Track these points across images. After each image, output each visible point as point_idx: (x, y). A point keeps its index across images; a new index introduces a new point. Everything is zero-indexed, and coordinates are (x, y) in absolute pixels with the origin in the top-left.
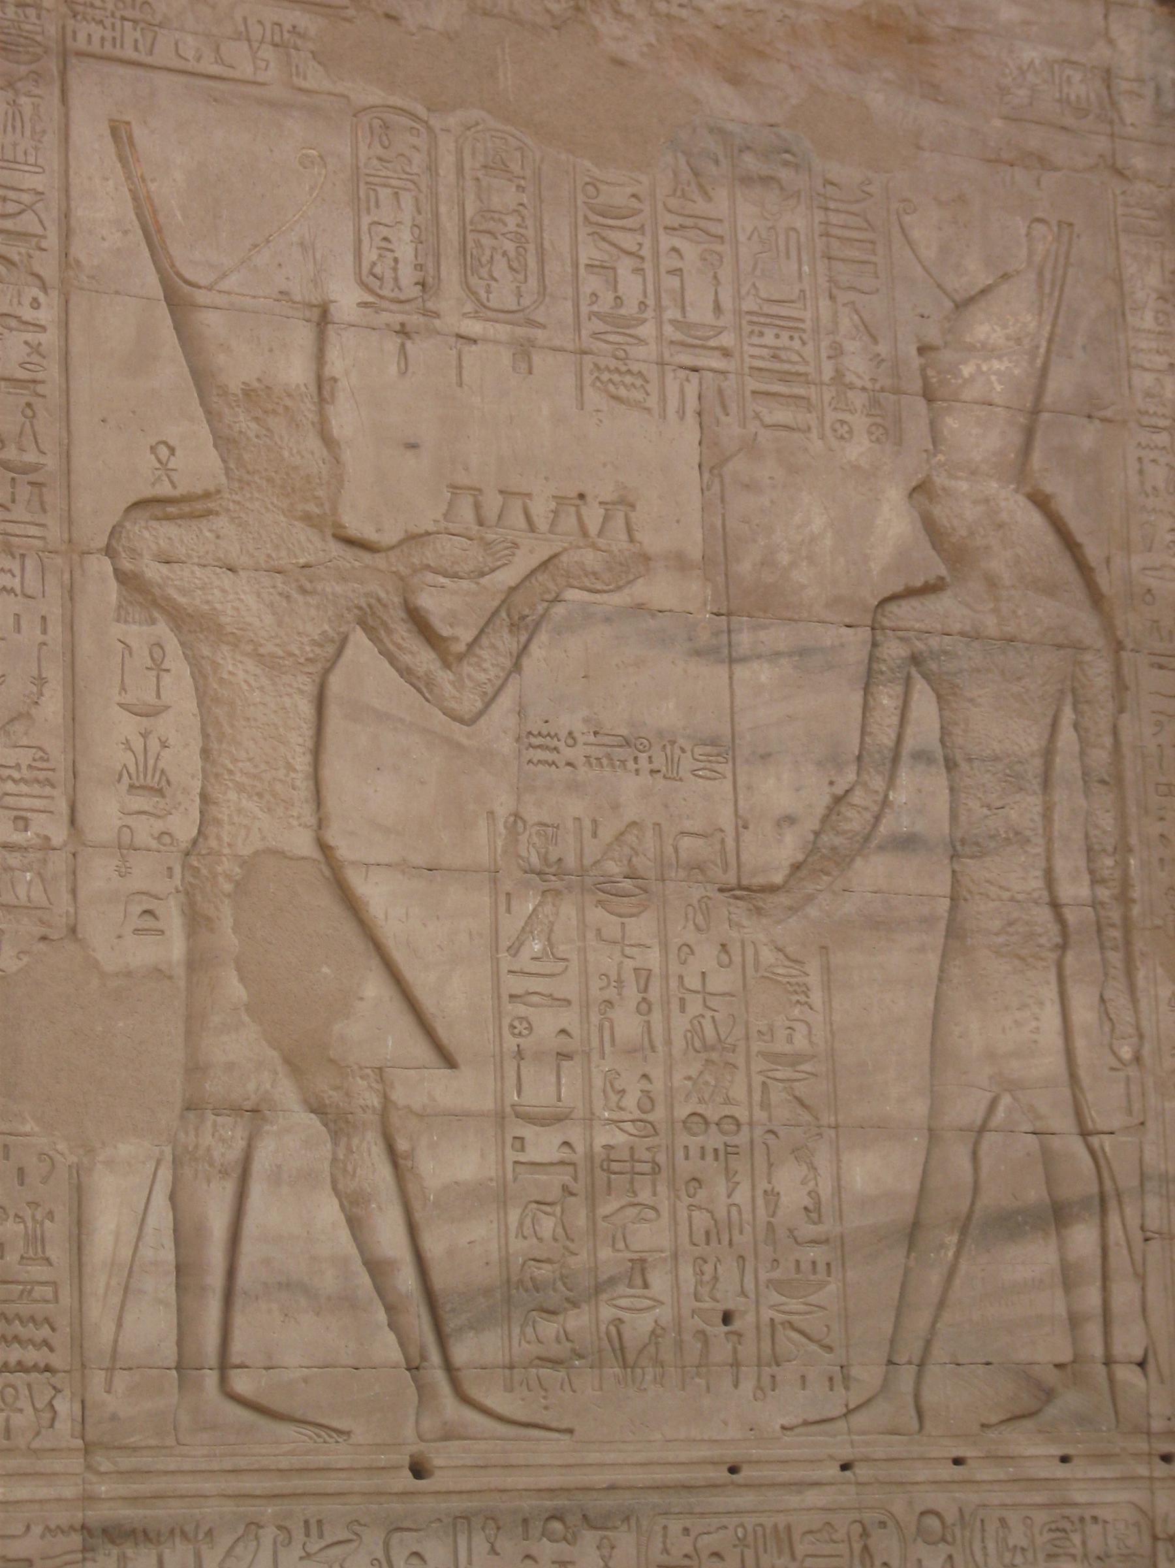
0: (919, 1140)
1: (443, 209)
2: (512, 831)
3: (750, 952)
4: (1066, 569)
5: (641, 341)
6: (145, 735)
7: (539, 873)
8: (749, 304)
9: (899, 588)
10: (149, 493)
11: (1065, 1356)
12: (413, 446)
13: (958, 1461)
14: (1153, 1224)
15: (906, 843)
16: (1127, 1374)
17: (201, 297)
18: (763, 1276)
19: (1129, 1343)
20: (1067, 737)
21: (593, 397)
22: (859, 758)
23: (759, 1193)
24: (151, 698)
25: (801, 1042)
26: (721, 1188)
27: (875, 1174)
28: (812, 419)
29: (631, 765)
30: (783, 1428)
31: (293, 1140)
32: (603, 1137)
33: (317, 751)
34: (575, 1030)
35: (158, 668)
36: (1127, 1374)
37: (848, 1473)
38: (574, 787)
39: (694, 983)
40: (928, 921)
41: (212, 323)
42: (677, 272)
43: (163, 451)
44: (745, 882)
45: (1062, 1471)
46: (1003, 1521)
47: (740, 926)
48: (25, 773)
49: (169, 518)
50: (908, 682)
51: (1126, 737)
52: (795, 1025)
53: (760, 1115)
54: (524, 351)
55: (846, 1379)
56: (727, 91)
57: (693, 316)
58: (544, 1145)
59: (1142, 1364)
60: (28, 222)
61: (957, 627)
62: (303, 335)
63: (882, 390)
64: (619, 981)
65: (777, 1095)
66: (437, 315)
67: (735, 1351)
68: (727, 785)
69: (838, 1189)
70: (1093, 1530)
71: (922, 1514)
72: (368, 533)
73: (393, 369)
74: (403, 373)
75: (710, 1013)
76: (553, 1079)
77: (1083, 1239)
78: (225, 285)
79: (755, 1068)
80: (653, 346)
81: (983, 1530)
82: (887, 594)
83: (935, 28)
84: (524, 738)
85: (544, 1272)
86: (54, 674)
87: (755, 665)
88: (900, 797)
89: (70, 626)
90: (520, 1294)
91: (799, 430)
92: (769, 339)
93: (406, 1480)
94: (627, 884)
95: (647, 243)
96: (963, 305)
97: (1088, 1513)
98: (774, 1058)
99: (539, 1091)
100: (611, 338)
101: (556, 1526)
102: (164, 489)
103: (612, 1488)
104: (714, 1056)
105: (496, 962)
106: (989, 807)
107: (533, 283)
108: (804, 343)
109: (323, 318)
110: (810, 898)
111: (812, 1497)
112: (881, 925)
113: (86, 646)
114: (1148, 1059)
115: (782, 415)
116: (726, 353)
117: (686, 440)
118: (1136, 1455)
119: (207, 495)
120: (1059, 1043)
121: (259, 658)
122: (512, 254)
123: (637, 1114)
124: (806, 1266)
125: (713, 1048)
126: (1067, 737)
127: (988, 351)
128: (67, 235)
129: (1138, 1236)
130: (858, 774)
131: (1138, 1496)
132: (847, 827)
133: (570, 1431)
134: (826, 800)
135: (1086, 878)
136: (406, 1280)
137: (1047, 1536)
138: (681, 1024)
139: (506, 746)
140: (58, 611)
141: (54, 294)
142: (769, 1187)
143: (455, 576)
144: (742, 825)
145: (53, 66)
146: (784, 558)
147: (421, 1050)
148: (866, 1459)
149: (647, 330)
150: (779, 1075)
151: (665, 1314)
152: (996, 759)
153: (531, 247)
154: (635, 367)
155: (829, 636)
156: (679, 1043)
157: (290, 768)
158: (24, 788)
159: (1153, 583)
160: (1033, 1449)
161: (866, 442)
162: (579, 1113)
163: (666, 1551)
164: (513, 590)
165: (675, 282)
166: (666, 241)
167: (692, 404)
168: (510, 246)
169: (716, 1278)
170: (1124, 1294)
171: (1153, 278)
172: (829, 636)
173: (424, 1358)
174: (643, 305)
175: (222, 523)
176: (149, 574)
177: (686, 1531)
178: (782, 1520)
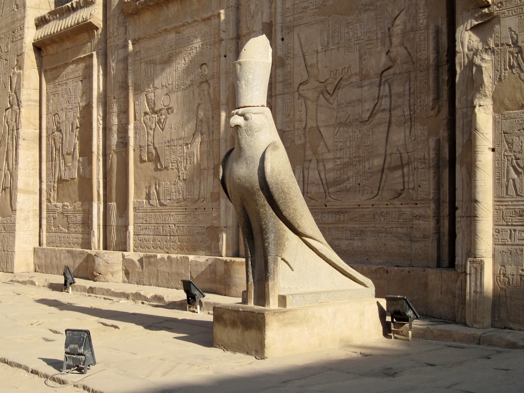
0: (383, 157)
2: (336, 118)
8: (366, 31)
9: (383, 69)
10: (300, 82)
11: (402, 188)
15: (383, 110)
17: (306, 54)
19: (411, 186)
20: (407, 87)
21: (346, 52)
22: (378, 98)
25: (369, 144)
27: (378, 162)
31: (313, 165)
35: (302, 105)
36: (411, 191)
38: (343, 111)
40: (386, 122)
41: (307, 57)
42: (356, 29)
45: (401, 206)
57: (358, 35)
58: (339, 162)
60: (290, 51)
62: (315, 55)
68: (361, 107)
69: (372, 165)
70: (405, 215)
77: (406, 170)
82: (382, 71)
85: (338, 179)
86: (292, 108)
88: (383, 103)
90: (336, 182)
93: (324, 207)
98: (365, 146)
99: (338, 155)
102: (302, 81)
109: (317, 52)
111: (368, 210)
112: (380, 124)
118: (411, 204)
127: (399, 25)
129: (413, 168)
130: (378, 100)
131: (411, 210)
136: (324, 181)
138: (354, 143)
139: (336, 107)
144: (362, 112)
146: (369, 69)
147: (327, 151)
149: (353, 40)
151: (351, 184)
155: (374, 80)
159: (421, 57)
160: (397, 202)
164: (337, 84)
168: (337, 33)
170: (411, 178)
171: (423, 3)
175: (309, 84)
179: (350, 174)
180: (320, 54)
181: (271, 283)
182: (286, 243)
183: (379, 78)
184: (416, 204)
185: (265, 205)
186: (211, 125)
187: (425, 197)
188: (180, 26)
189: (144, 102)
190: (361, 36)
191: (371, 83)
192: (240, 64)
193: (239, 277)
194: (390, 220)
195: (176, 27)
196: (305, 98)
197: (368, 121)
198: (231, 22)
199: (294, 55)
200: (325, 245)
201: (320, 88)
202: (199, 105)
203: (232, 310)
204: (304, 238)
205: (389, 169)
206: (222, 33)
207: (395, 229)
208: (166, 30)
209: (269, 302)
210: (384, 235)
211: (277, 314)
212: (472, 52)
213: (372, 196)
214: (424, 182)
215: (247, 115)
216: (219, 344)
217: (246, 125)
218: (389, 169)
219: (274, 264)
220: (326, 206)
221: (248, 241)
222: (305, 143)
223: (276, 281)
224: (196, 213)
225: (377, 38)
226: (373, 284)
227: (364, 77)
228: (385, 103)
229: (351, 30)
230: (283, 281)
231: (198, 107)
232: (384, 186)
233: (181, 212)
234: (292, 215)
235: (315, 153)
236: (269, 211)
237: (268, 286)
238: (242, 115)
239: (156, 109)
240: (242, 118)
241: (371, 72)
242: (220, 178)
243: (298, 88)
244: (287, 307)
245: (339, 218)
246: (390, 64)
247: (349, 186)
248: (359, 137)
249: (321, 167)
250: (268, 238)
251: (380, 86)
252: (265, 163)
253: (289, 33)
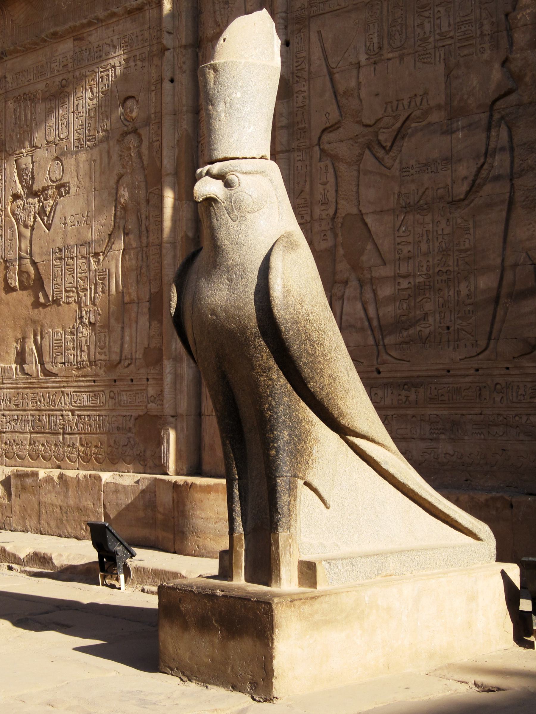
0: (498, 271)
1: (384, 24)
2: (399, 196)
3: (454, 220)
5: (430, 43)
6: (324, 190)
7: (405, 208)
8: (458, 20)
9: (496, 96)
10: (324, 127)
12: (377, 95)
13: (508, 368)
15: (497, 178)
17: (335, 71)
18: (456, 316)
23: (456, 291)
24: (325, 180)
25: (467, 246)
26: (446, 292)
27: (486, 282)
29: (427, 171)
30: (460, 359)
32: (417, 280)
33: (358, 185)
34: (412, 251)
35: (327, 172)
37: (477, 373)
38: (413, 181)
42: (439, 18)
43: (327, 115)
44: (454, 200)
46: (518, 386)
48: (303, 205)
49: (331, 132)
50: (500, 126)
52: (466, 240)
53: (456, 268)
54: (401, 58)
55: (477, 345)
57: (443, 30)
58: (404, 284)
60: (303, 66)
61: (514, 103)
62: (355, 72)
63: (494, 33)
64: (422, 235)
65: (460, 262)
66: (382, 55)
67: (449, 338)
68: (450, 171)
69: (476, 288)
71: (497, 384)
72: (368, 122)
73: (373, 74)
74: (375, 75)
75: (444, 241)
76: (406, 265)
78: (339, 66)
79: (455, 255)
80: (433, 44)
81: (512, 389)
84: (402, 170)
85: (404, 318)
86: (308, 179)
87: (457, 133)
88: (496, 164)
89: (310, 165)
90: (399, 324)
91: (470, 55)
93: (375, 374)
94: (425, 206)
95: (432, 12)
98: (461, 251)
99: (403, 270)
100: (422, 45)
101: (406, 387)
102: (328, 125)
103: (419, 377)
104: (445, 253)
105: (394, 234)
106: (522, 160)
107: (404, 36)
108: (472, 26)
109: (358, 66)
111: (467, 379)
113: (314, 170)
115: (466, 52)
117: (441, 68)
119: (336, 124)
121: (346, 163)
122: (400, 30)
123: (426, 272)
124: (467, 312)
125: (444, 251)
127: (527, 7)
128: (310, 65)
132: (482, 176)
133: (409, 361)
134: (476, 169)
136: (375, 323)
137: (531, 391)
138: (437, 244)
139: (397, 173)
140: (309, 163)
141: (307, 82)
142: (457, 289)
143: (388, 128)
144: (453, 182)
145: (307, 23)
146: (466, 97)
147: (379, 261)
148: (481, 368)
149: (431, 39)
150: (461, 256)
151: (432, 328)
152: (525, 144)
153: (404, 26)
154: (428, 52)
156: (436, 250)
157: (352, 191)
158: (303, 209)
161: (489, 52)
162: (412, 274)
163: (431, 394)
165: (438, 21)
166: (436, 9)
167: (443, 56)
168: (399, 28)
169: (444, 317)
173: (379, 343)
174: (430, 31)
175: (341, 129)
176: (326, 148)
177: (436, 388)
179: (429, 307)
180: (363, 70)
181: (282, 535)
182: (314, 451)
183: (487, 114)
185: (270, 369)
186: (143, 217)
188: (83, 26)
189: (12, 174)
190: (449, 31)
191: (470, 125)
192: (215, 69)
193: (203, 516)
195: (74, 29)
196: (335, 158)
197: (464, 200)
198: (183, 14)
199: (310, 73)
200: (394, 453)
201: (364, 136)
202: (120, 177)
203: (199, 593)
204: (351, 438)
205: (510, 295)
206: (166, 35)
207: (524, 418)
208: (55, 35)
209: (279, 576)
211: (297, 603)
215: (230, 177)
216: (173, 665)
217: (229, 199)
218: (510, 295)
219: (290, 495)
220: (379, 372)
221: (232, 445)
222: (335, 246)
223: (293, 530)
224: (116, 390)
225: (482, 35)
226: (492, 534)
227: (454, 111)
228: (500, 163)
229: (427, 20)
230: (307, 530)
231: (118, 181)
232: (500, 331)
233: (85, 387)
234: (326, 390)
235: (356, 267)
236: (280, 382)
237: (277, 541)
238: (221, 177)
239: (35, 188)
240: (220, 183)
241: (469, 102)
242: (173, 311)
243: (320, 138)
244: (319, 587)
245: (407, 397)
247: (427, 331)
248: (446, 232)
249: (369, 296)
250: (276, 439)
251: (489, 129)
252: (271, 277)
253: (300, 31)
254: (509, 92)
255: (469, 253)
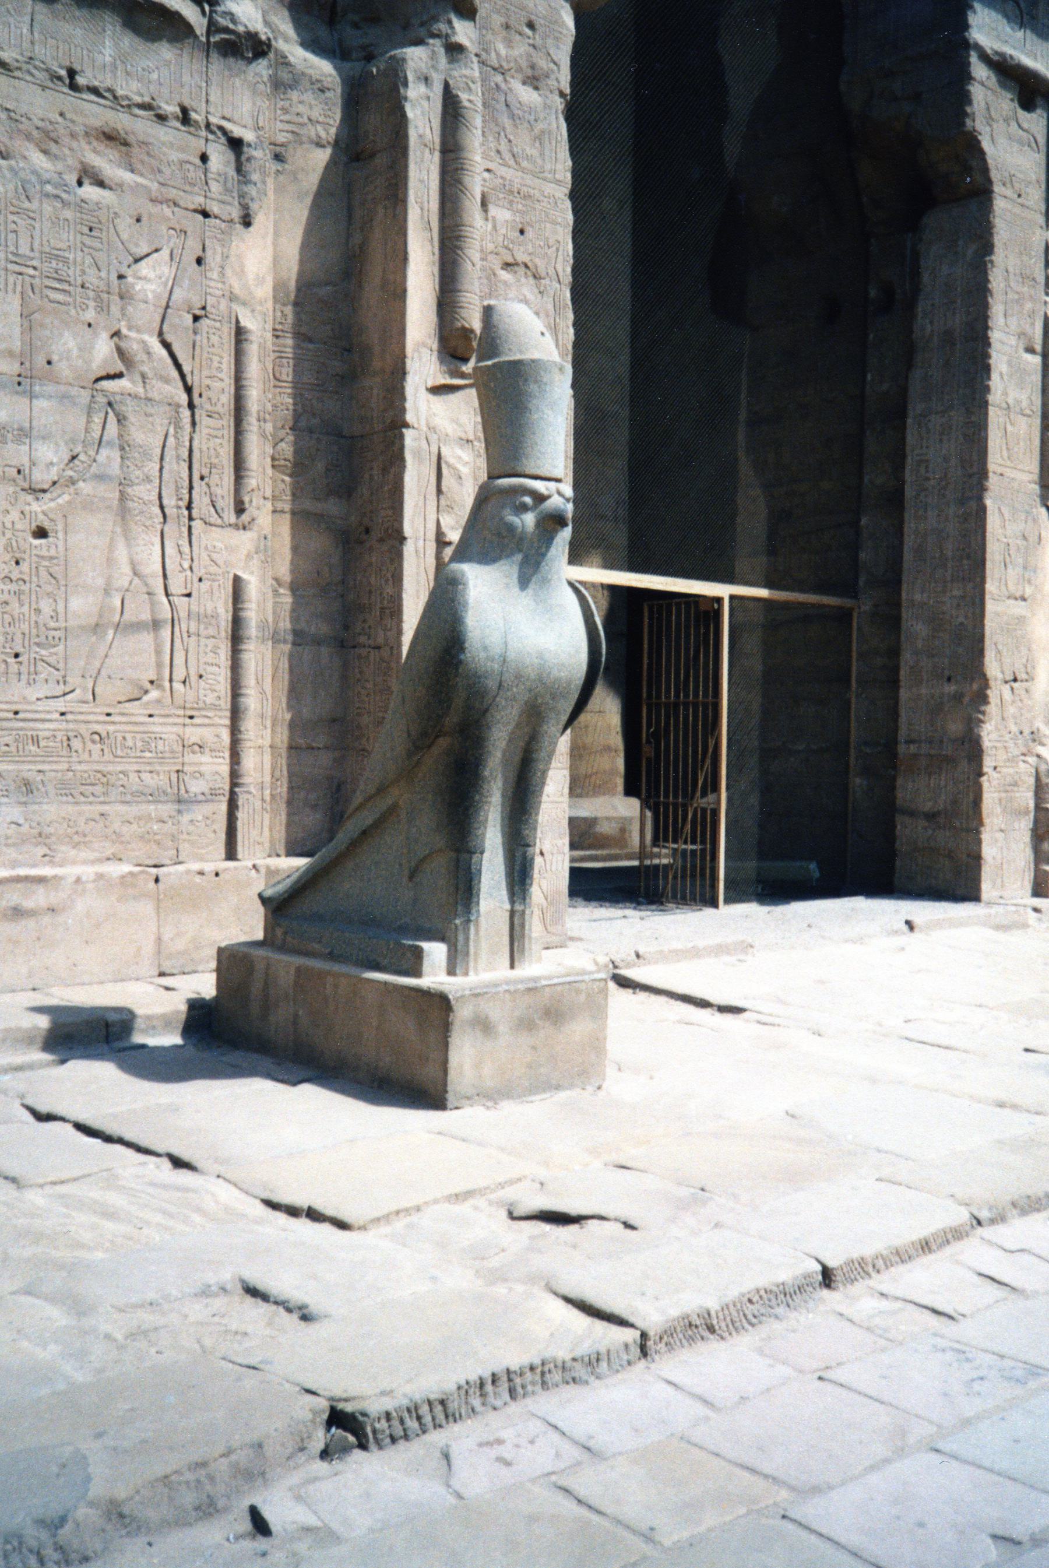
4: (175, 374)
13: (108, 715)
14: (192, 630)
15: (100, 478)
16: (178, 686)
25: (53, 552)
28: (71, 300)
39: (9, 525)
46: (124, 738)
47: (29, 504)
51: (195, 443)
53: (35, 579)
56: (42, 156)
59: (184, 682)
65: (43, 572)
68: (27, 448)
70: (161, 742)
83: (131, 139)
92: (54, 262)
96: (137, 261)
97: (158, 736)
98: (42, 557)
110: (59, 496)
111: (47, 725)
114: (194, 569)
116: (35, 268)
120: (160, 559)
126: (171, 440)
129: (185, 635)
131: (179, 730)
135: (175, 498)
146: (55, 358)
148: (71, 712)
167: (19, 288)
172: (74, 391)
178: (34, 733)
184: (191, 717)
187: (217, 703)
190: (32, 259)
194: (119, 753)
210: (98, 789)
212: (435, 437)
213: (60, 689)
214: (215, 669)
246: (123, 369)
254: (119, 375)
255: (55, 561)
